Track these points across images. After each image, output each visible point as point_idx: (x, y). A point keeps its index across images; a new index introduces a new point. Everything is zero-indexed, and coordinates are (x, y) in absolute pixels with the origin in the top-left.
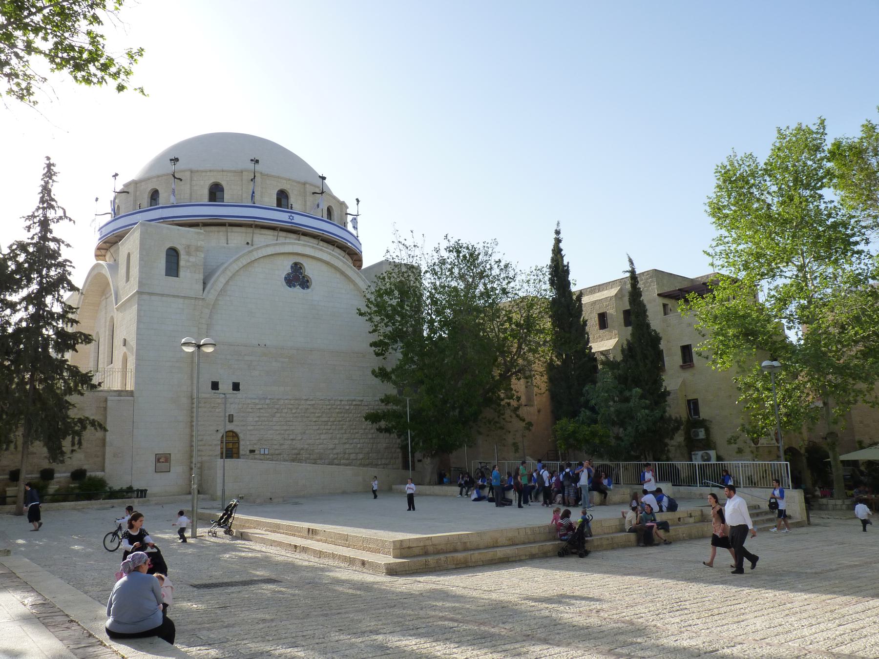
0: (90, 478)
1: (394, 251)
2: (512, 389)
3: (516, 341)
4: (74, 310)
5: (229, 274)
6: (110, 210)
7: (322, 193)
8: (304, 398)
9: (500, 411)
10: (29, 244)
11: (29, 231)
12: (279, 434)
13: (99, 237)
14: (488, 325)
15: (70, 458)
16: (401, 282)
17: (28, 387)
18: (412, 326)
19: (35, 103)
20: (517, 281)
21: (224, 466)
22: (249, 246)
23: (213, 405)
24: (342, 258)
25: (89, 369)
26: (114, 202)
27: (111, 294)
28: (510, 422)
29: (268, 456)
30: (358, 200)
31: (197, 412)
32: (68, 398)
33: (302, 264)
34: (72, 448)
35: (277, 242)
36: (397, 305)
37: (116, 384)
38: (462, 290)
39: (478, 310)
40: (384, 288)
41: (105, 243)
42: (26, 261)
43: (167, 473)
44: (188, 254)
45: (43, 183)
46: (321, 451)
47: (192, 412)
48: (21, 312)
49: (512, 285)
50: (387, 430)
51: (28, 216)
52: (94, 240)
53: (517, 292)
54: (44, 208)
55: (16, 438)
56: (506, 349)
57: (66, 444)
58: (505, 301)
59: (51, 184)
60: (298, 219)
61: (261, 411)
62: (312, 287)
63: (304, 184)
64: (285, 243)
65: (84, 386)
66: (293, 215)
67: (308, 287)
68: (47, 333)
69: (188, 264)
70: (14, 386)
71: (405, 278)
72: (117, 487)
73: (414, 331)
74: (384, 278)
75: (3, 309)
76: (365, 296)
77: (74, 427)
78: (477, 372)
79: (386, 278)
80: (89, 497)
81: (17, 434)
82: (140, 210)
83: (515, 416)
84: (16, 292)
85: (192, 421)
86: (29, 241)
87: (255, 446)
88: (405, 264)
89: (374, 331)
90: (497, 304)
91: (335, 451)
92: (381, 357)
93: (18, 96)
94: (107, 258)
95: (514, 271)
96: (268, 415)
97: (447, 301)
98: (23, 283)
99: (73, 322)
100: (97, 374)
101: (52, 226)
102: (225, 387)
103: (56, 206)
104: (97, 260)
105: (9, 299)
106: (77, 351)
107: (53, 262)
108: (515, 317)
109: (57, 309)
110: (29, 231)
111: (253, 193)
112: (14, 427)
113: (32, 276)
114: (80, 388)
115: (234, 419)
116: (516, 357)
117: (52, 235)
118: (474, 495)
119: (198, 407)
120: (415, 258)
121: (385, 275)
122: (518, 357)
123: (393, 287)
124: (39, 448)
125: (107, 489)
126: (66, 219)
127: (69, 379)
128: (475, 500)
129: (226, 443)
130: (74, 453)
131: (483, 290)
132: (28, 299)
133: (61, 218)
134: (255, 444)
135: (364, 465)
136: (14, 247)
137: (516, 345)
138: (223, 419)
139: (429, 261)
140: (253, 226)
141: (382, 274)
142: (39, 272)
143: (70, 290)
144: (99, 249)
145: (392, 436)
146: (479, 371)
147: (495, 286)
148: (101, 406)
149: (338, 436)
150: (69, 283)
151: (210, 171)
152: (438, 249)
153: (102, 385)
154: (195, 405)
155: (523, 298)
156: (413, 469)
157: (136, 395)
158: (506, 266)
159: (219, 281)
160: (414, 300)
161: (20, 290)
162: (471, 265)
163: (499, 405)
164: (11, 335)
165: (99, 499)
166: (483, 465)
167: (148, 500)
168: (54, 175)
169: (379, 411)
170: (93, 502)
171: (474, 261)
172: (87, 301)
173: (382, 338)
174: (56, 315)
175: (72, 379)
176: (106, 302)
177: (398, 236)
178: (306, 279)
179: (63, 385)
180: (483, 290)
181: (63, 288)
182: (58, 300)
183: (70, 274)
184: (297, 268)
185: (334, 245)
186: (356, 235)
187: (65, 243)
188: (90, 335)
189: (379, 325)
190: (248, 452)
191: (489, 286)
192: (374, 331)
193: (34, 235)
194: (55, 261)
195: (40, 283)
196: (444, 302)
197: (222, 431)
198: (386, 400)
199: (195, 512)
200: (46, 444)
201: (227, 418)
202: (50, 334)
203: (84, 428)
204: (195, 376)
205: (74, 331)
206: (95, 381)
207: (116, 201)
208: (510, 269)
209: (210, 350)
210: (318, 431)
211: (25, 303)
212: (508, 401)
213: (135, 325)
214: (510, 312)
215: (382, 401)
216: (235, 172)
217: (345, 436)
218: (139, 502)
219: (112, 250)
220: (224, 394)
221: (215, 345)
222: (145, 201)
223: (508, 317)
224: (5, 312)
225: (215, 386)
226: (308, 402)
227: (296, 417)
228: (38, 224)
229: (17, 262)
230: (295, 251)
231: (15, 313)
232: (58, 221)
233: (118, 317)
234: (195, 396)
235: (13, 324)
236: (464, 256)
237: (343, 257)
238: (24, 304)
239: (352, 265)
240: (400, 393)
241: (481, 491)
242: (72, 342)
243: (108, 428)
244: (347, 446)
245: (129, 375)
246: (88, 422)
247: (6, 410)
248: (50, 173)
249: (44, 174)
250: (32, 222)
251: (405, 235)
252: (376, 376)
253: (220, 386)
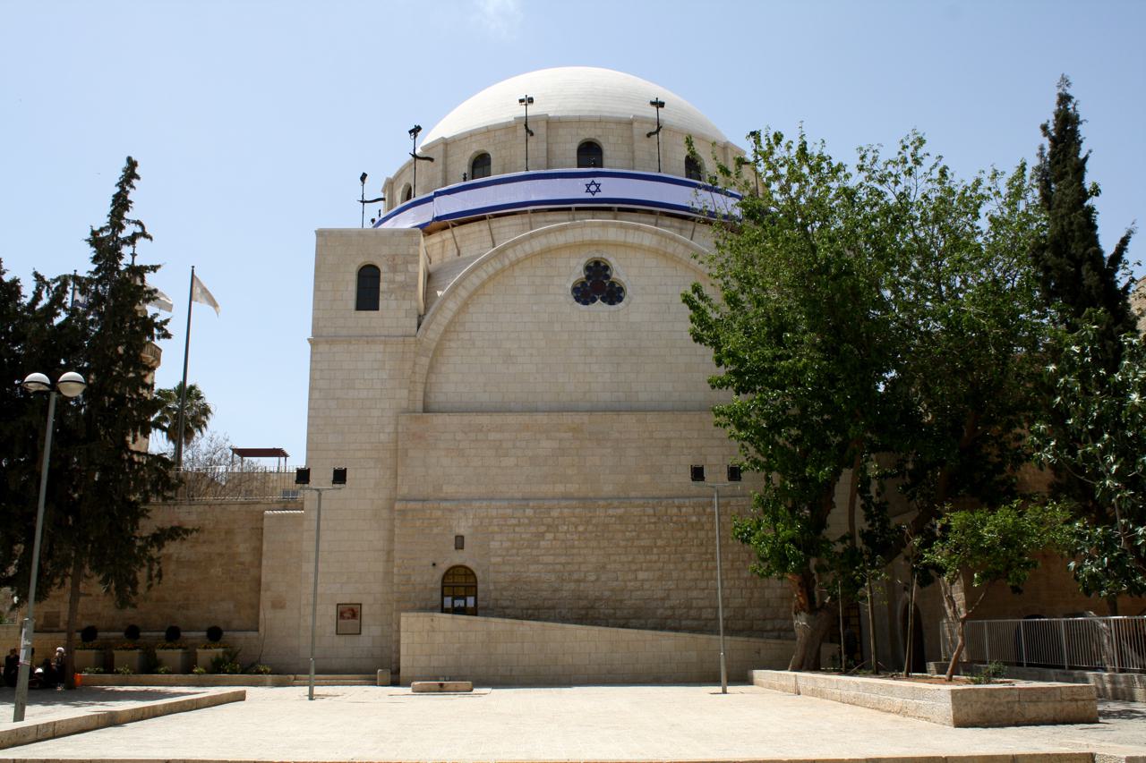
43: (356, 637)
67: (620, 299)
69: (391, 286)
149: (675, 575)
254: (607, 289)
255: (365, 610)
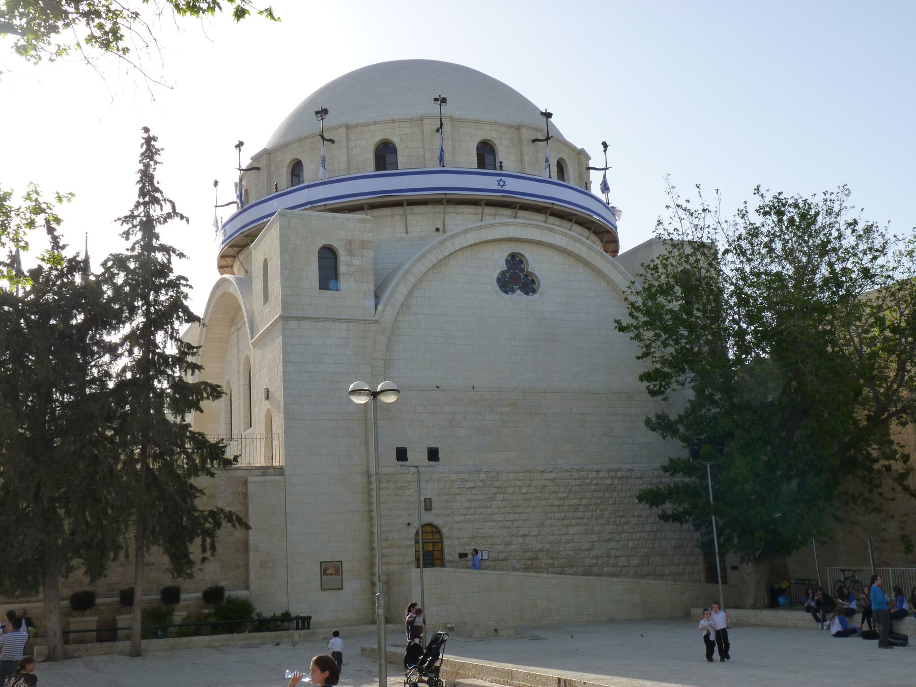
0: (230, 601)
1: (671, 221)
2: (891, 442)
3: (893, 357)
4: (195, 350)
5: (412, 279)
6: (234, 198)
7: (548, 138)
8: (539, 469)
9: (872, 479)
10: (128, 258)
11: (127, 239)
12: (504, 527)
13: (221, 238)
14: (841, 333)
15: (201, 570)
16: (684, 271)
17: (139, 466)
18: (707, 343)
19: (126, 50)
20: (890, 254)
21: (422, 580)
22: (441, 233)
23: (400, 485)
24: (584, 239)
25: (220, 437)
26: (239, 185)
27: (245, 323)
28: (893, 499)
29: (488, 563)
30: (605, 145)
31: (378, 496)
32: (193, 481)
33: (522, 255)
34: (203, 556)
35: (484, 223)
36: (680, 310)
37: (259, 459)
38: (790, 277)
39: (821, 309)
40: (656, 284)
41: (231, 247)
42: (126, 283)
44: (351, 253)
45: (141, 167)
46: (570, 553)
47: (370, 496)
48: (123, 358)
49: (881, 261)
50: (676, 518)
51: (126, 217)
52: (214, 245)
53: (891, 273)
54: (145, 204)
55: (127, 543)
56: (875, 372)
57: (195, 548)
58: (869, 290)
59: (153, 167)
60: (512, 185)
61: (474, 491)
62: (540, 291)
63: (519, 128)
64: (493, 225)
65: (215, 462)
66: (504, 179)
67: (534, 291)
68: (159, 386)
70: (119, 467)
71: (690, 264)
72: (267, 614)
73: (713, 352)
74: (656, 268)
75: (99, 354)
76: (626, 299)
77: (204, 524)
78: (826, 415)
79: (660, 266)
80: (230, 629)
81: (127, 535)
82: (278, 193)
83: (900, 488)
84: (115, 328)
85: (370, 511)
86: (129, 253)
87: (467, 547)
88: (689, 242)
89: (645, 355)
90: (855, 297)
91: (593, 553)
92: (660, 397)
93: (102, 44)
94: (235, 269)
95: (883, 236)
96: (483, 497)
97: (765, 299)
98: (124, 315)
99: (195, 367)
100: (232, 443)
101: (159, 229)
102: (417, 456)
103: (161, 199)
104: (222, 274)
105: (107, 341)
106: (202, 411)
107: (162, 281)
108: (890, 316)
109: (171, 350)
110: (127, 239)
111: (442, 150)
112: (123, 526)
113: (136, 304)
114: (209, 466)
115: (433, 505)
116: (895, 386)
117: (159, 242)
118: (836, 627)
119: (379, 489)
120: (706, 230)
121: (657, 262)
122: (899, 386)
123: (672, 281)
124: (158, 556)
125: (254, 616)
126: (176, 217)
127: (193, 452)
128: (838, 635)
129: (423, 543)
130: (206, 562)
131: (827, 274)
132: (132, 338)
133: (169, 216)
134: (467, 544)
135: (643, 576)
136: (110, 264)
137: (894, 365)
138: (416, 505)
139: (731, 234)
140: (445, 203)
141: (653, 261)
142: (145, 298)
143: (187, 321)
144: (223, 256)
145: (685, 527)
146: (829, 414)
147: (849, 265)
148: (240, 491)
149: (597, 528)
150: (186, 310)
151: (375, 123)
152: (744, 212)
153: (239, 459)
154: (374, 486)
155: (902, 284)
156: (725, 582)
157: (287, 472)
158: (868, 230)
159: (398, 292)
160: (708, 300)
161: (121, 326)
162: (804, 233)
163: (871, 470)
164: (113, 391)
165: (244, 631)
166: (847, 574)
167: (313, 632)
168: (156, 153)
169: (661, 487)
170: (236, 636)
171: (809, 225)
172: (211, 335)
173: (658, 366)
174: (170, 360)
175: (198, 452)
176: (238, 336)
177: (675, 197)
178: (530, 278)
179: (185, 461)
180: (827, 274)
181: (178, 318)
182: (172, 337)
183: (186, 297)
184: (515, 261)
185: (570, 220)
186: (605, 201)
187: (177, 252)
188: (219, 386)
189: (653, 345)
190: (457, 556)
191: (838, 267)
192: (645, 355)
193: (135, 244)
194: (165, 280)
195: (147, 314)
196: (760, 300)
197: (416, 525)
198: (673, 467)
199: (383, 651)
200: (167, 551)
201: (423, 504)
202: (164, 387)
203: (218, 525)
204: (372, 440)
205: (196, 381)
206: (229, 454)
207: (243, 183)
208: (876, 235)
209: (390, 399)
210: (565, 522)
211: (129, 344)
212: (885, 462)
213: (281, 367)
214: (880, 308)
215: (665, 469)
216: (411, 120)
217: (609, 528)
218: (300, 636)
219: (241, 257)
220: (416, 467)
221: (397, 391)
222: (283, 178)
223: (876, 318)
224: (102, 359)
225: (402, 454)
226: (546, 476)
227: (528, 499)
228: (138, 227)
229: (114, 286)
230: (511, 235)
231: (115, 360)
232: (165, 221)
233: (256, 356)
234: (373, 471)
235: (114, 375)
236: (791, 221)
237: (588, 238)
238: (127, 346)
239: (602, 250)
240: (695, 454)
241: (847, 619)
242: (194, 397)
243: (251, 524)
244: (612, 545)
245: (276, 443)
246: (222, 515)
247: (111, 501)
248: (150, 151)
249: (143, 154)
250: (130, 225)
251: (686, 193)
252: (653, 429)
253: (409, 455)
254: (523, 281)
255: (345, 566)
